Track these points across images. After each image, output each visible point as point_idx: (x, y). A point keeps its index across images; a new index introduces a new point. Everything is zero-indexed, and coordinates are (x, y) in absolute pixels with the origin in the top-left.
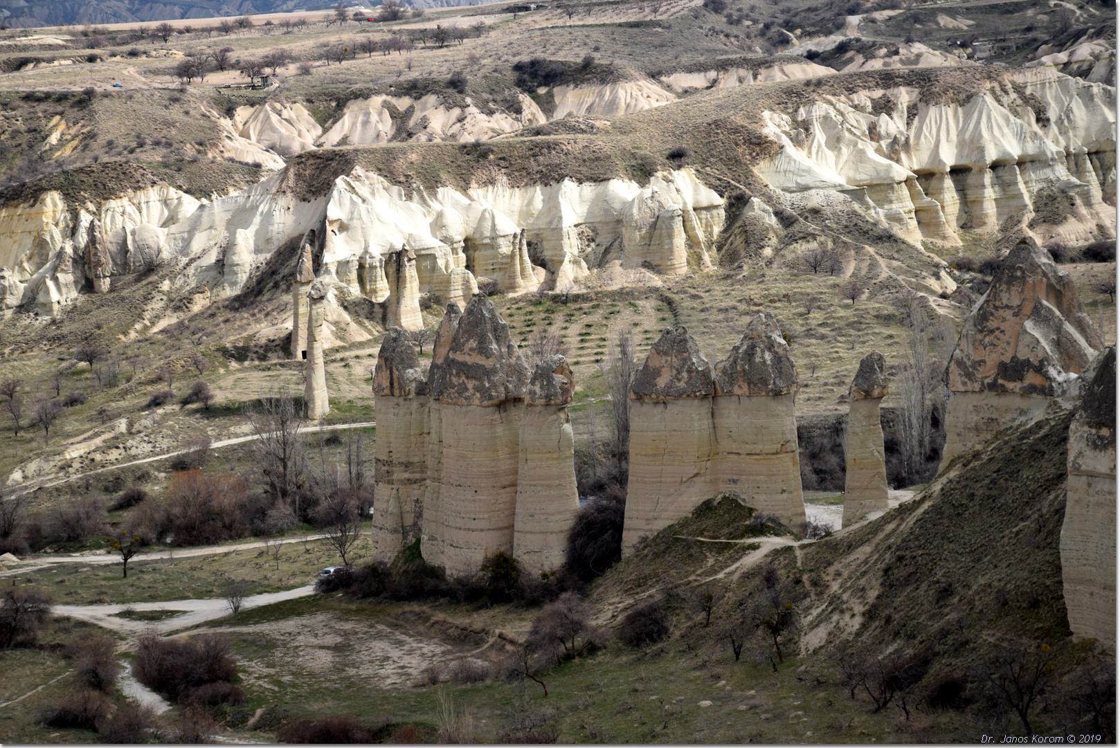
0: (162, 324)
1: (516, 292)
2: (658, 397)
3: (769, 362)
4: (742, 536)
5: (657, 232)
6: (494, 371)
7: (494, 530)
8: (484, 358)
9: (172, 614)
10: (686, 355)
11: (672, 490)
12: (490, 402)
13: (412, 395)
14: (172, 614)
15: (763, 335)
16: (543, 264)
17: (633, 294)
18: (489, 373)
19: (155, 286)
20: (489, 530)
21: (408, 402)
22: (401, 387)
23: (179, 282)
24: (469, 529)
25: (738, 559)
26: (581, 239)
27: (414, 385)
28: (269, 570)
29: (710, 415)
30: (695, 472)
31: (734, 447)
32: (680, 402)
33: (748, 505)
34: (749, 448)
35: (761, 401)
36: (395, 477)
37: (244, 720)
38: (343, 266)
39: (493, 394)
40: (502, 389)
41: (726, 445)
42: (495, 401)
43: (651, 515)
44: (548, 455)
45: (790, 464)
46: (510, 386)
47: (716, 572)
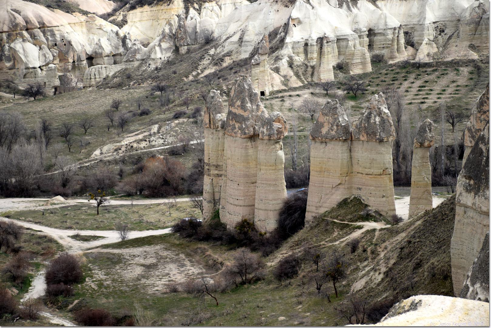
0: (207, 72)
1: (394, 60)
2: (322, 139)
3: (378, 123)
4: (356, 221)
5: (480, 27)
6: (247, 119)
7: (246, 206)
8: (243, 111)
9: (95, 238)
10: (336, 116)
11: (328, 191)
12: (245, 136)
13: (219, 129)
14: (95, 238)
15: (376, 107)
16: (412, 45)
17: (458, 64)
18: (245, 119)
19: (207, 51)
20: (244, 206)
21: (218, 132)
22: (214, 124)
23: (219, 50)
24: (235, 205)
25: (349, 234)
26: (436, 30)
27: (220, 123)
28: (152, 217)
29: (348, 151)
30: (339, 182)
31: (361, 170)
32: (333, 142)
33: (366, 203)
34: (367, 171)
35: (374, 144)
36: (211, 172)
37: (67, 306)
38: (295, 44)
39: (246, 131)
40: (252, 129)
41: (356, 168)
42: (247, 136)
43: (318, 205)
44: (270, 167)
45: (388, 181)
46: (257, 128)
47: (336, 241)
